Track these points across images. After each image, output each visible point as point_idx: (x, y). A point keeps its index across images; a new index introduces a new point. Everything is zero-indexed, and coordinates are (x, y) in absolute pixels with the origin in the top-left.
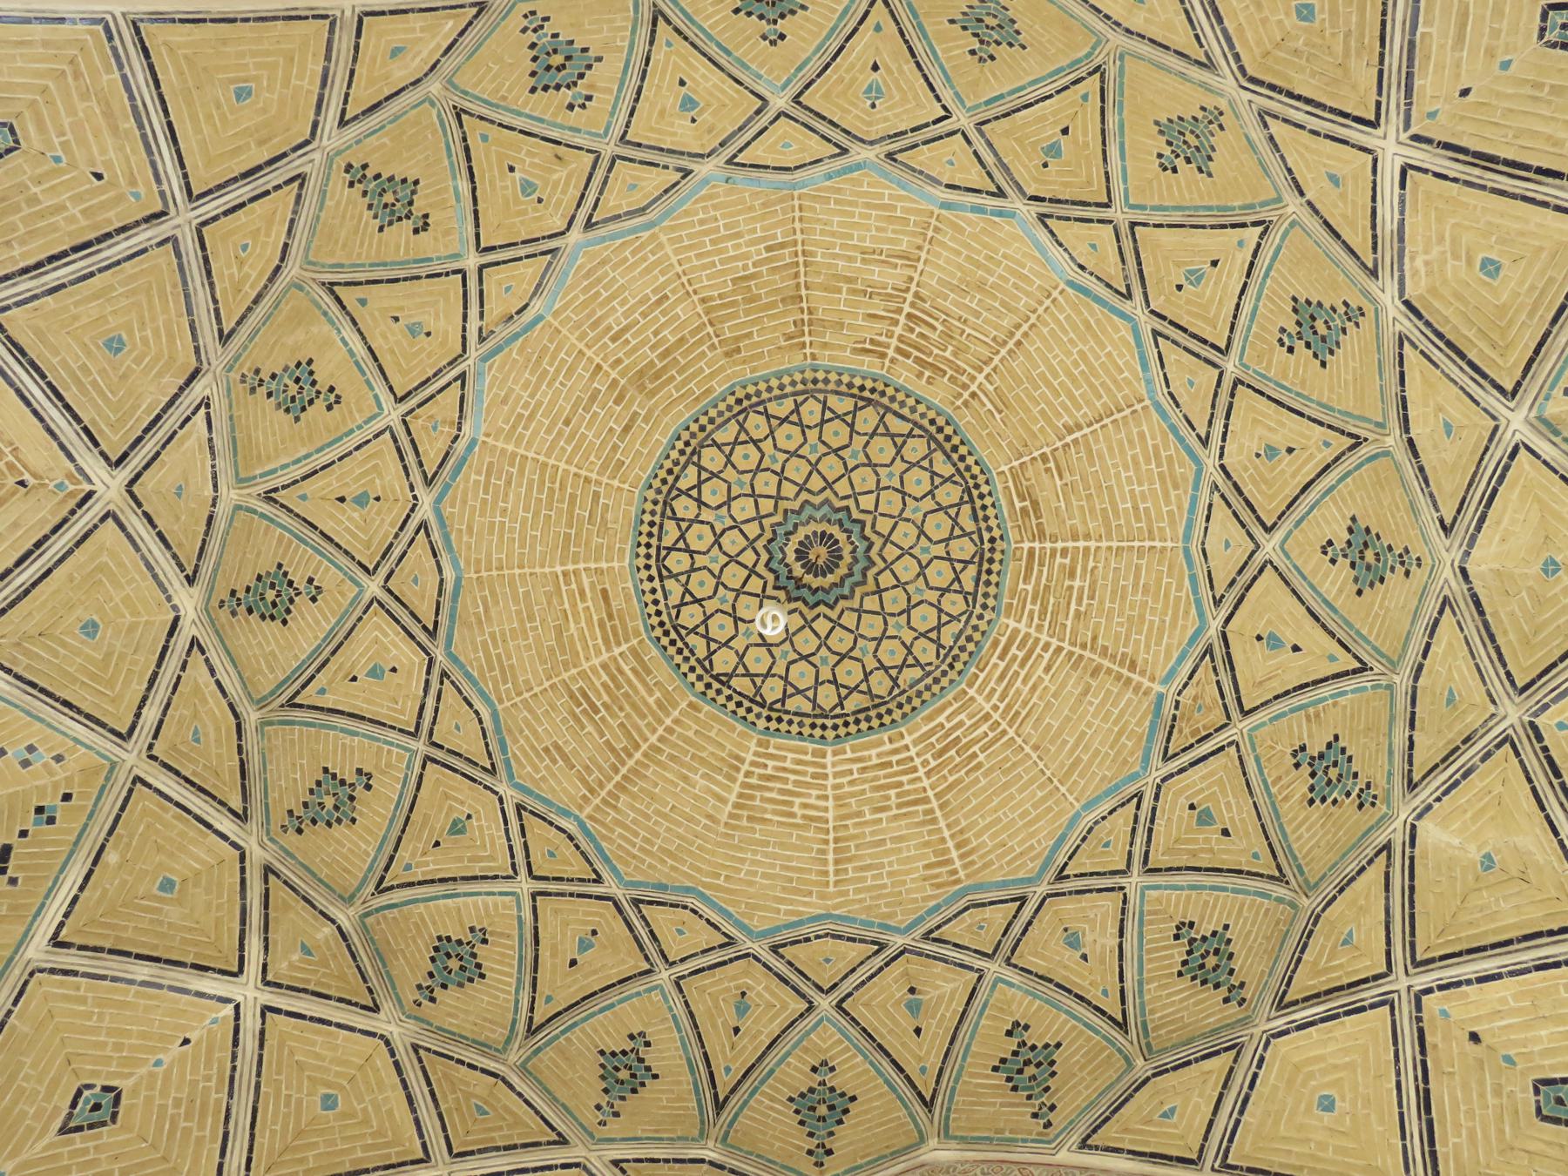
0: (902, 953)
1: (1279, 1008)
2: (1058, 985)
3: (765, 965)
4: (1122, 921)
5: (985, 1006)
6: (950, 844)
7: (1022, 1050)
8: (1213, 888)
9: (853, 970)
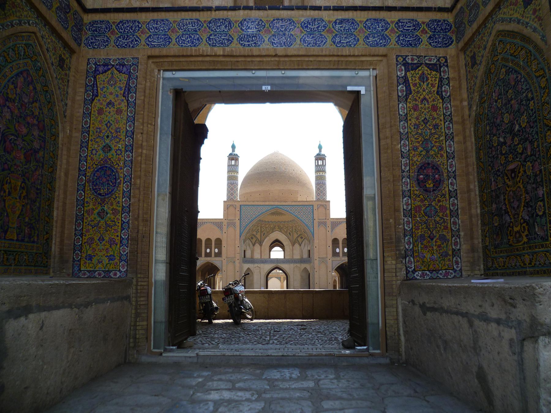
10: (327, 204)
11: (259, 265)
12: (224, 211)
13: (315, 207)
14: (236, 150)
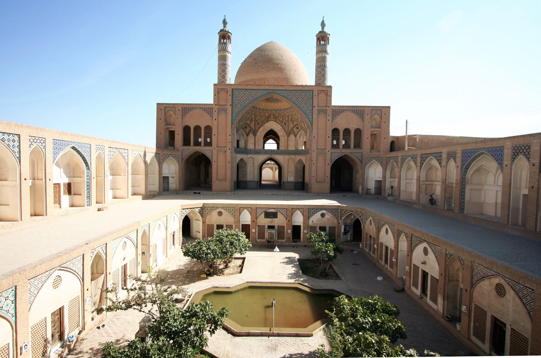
10: (328, 89)
11: (253, 156)
12: (215, 95)
13: (315, 93)
14: (227, 26)
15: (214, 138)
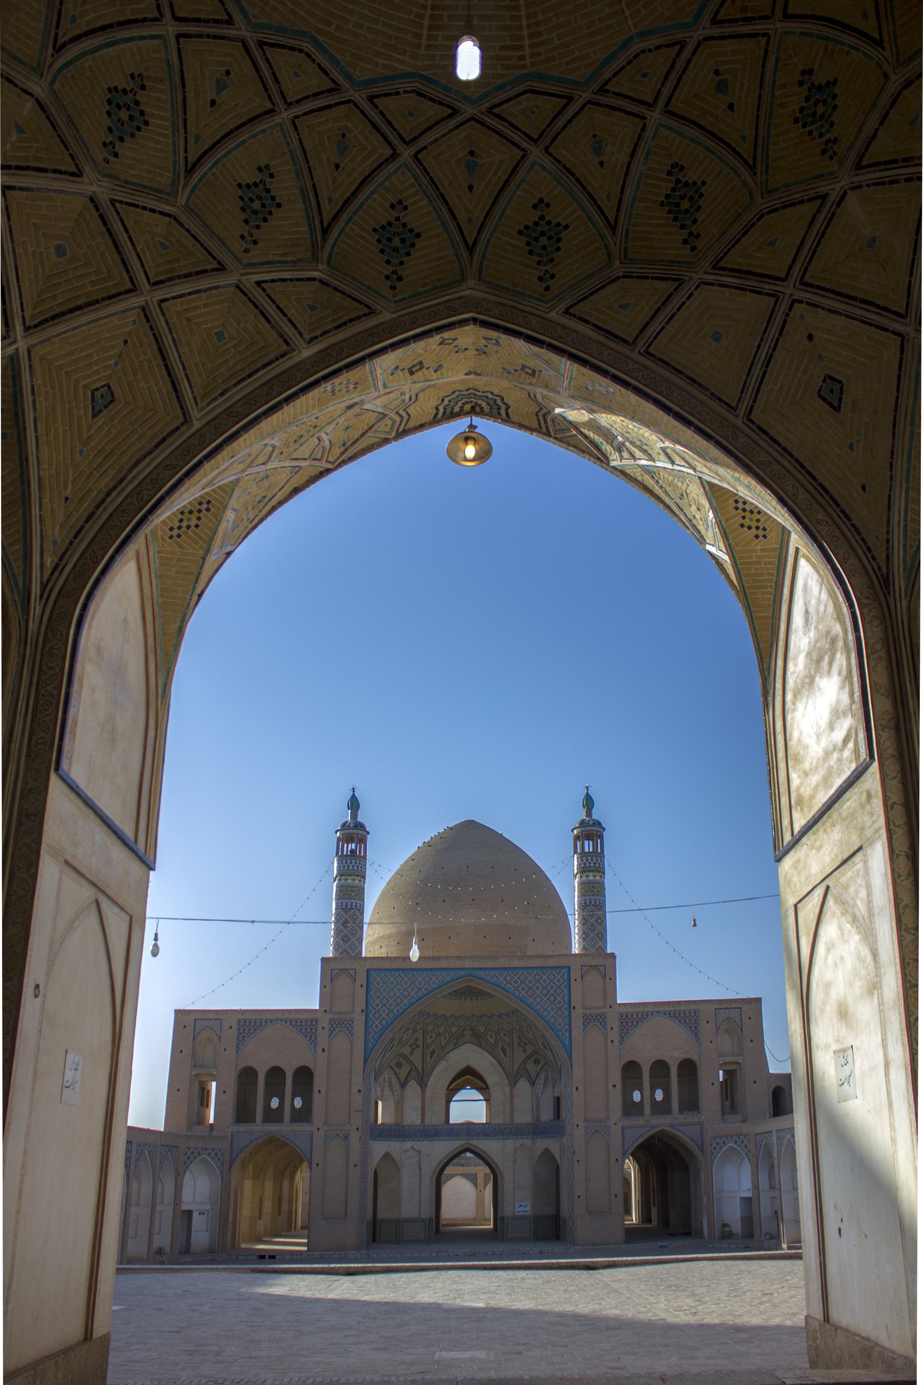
0: (469, 120)
1: (713, 268)
2: (578, 180)
3: (362, 112)
4: (636, 145)
5: (522, 181)
6: (525, 32)
7: (542, 222)
8: (706, 148)
9: (430, 128)
11: (417, 1145)
12: (323, 986)
13: (575, 973)
15: (318, 1101)
